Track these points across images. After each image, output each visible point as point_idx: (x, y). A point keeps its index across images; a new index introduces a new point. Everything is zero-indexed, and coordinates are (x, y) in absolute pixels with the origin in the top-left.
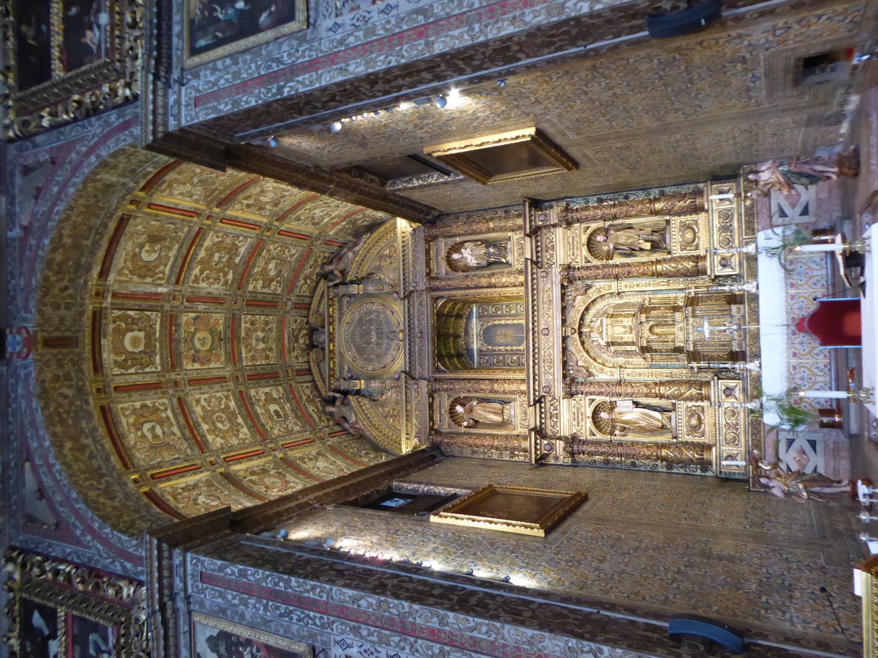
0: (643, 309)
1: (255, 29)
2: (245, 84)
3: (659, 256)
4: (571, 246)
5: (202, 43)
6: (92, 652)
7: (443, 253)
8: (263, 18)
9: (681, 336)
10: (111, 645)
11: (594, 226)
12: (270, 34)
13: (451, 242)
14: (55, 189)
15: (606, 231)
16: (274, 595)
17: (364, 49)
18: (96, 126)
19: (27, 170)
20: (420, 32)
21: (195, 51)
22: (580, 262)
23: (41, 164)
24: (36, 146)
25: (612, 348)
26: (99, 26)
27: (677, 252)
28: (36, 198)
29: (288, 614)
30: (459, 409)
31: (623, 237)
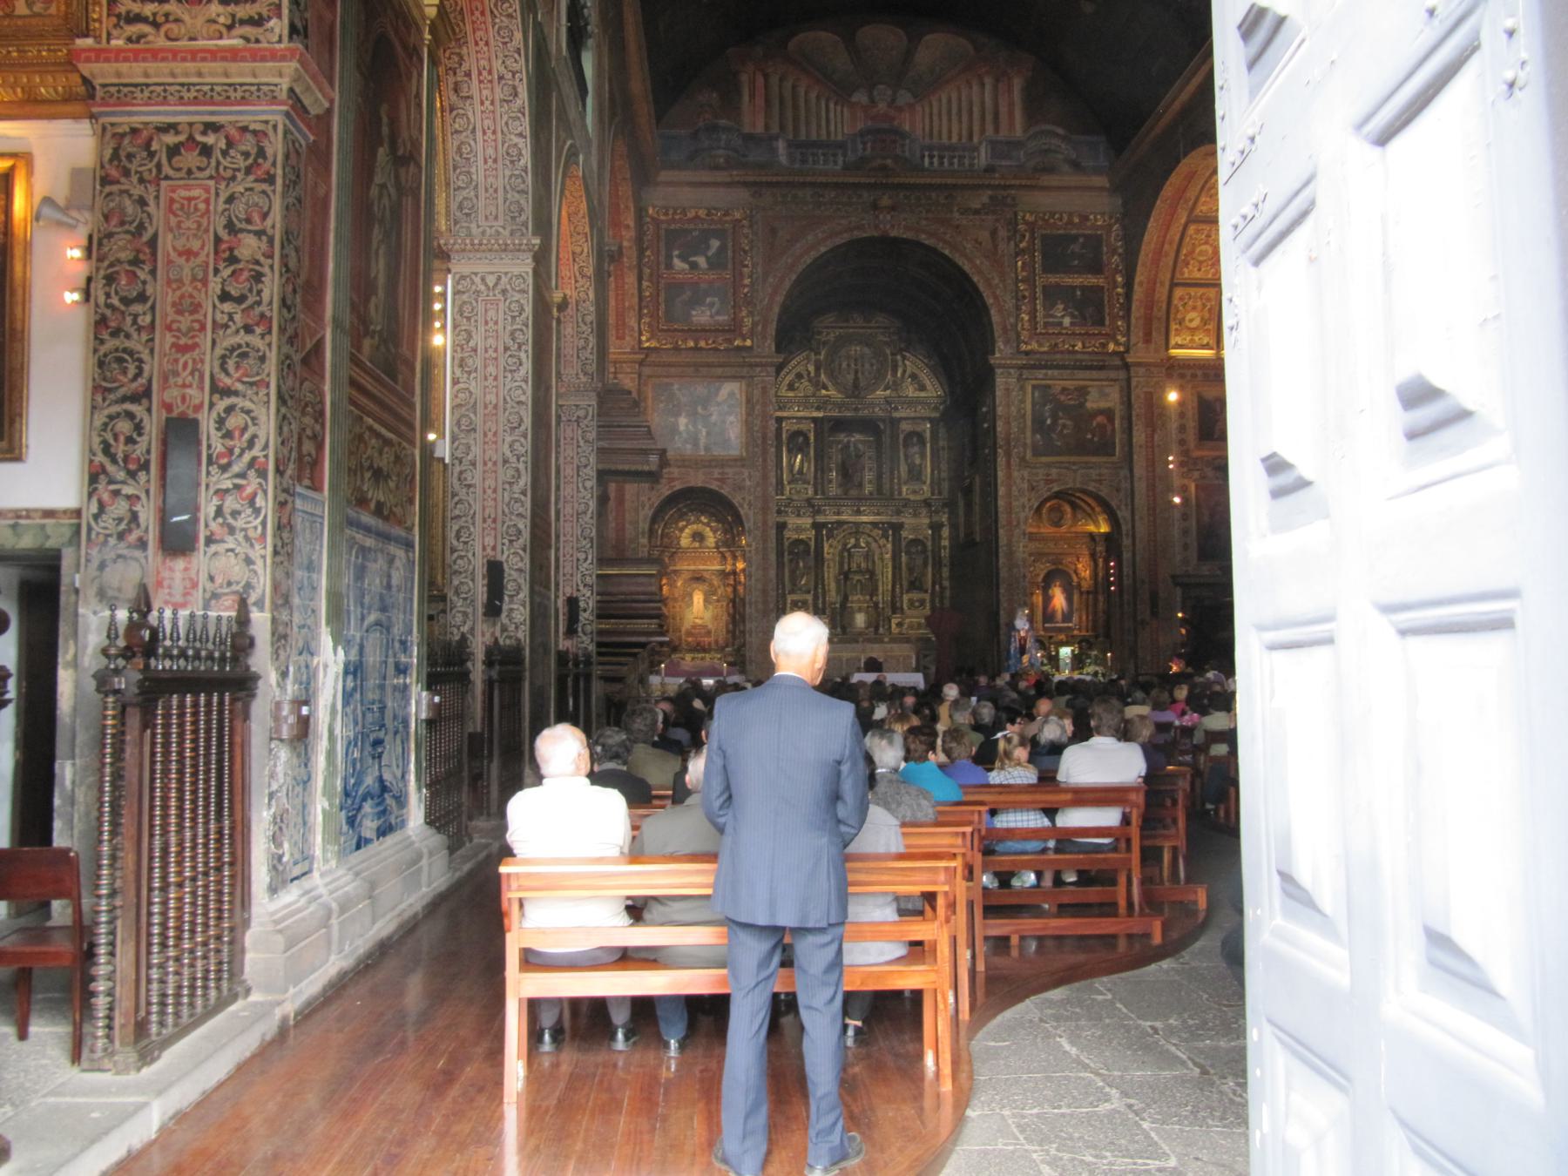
0: (872, 573)
1: (1034, 432)
2: (1009, 423)
3: (905, 583)
4: (915, 529)
5: (1036, 394)
6: (708, 300)
7: (919, 429)
8: (1038, 436)
9: (855, 598)
10: (717, 318)
11: (929, 544)
12: (1029, 441)
13: (928, 435)
14: (978, 262)
15: (924, 551)
16: (764, 438)
17: (1009, 494)
18: (1010, 304)
19: (994, 233)
20: (1010, 523)
21: (1034, 387)
22: (904, 534)
23: (996, 247)
24: (1009, 239)
25: (846, 554)
26: (1063, 317)
27: (906, 597)
28: (976, 241)
29: (757, 446)
30: (801, 439)
31: (919, 561)
